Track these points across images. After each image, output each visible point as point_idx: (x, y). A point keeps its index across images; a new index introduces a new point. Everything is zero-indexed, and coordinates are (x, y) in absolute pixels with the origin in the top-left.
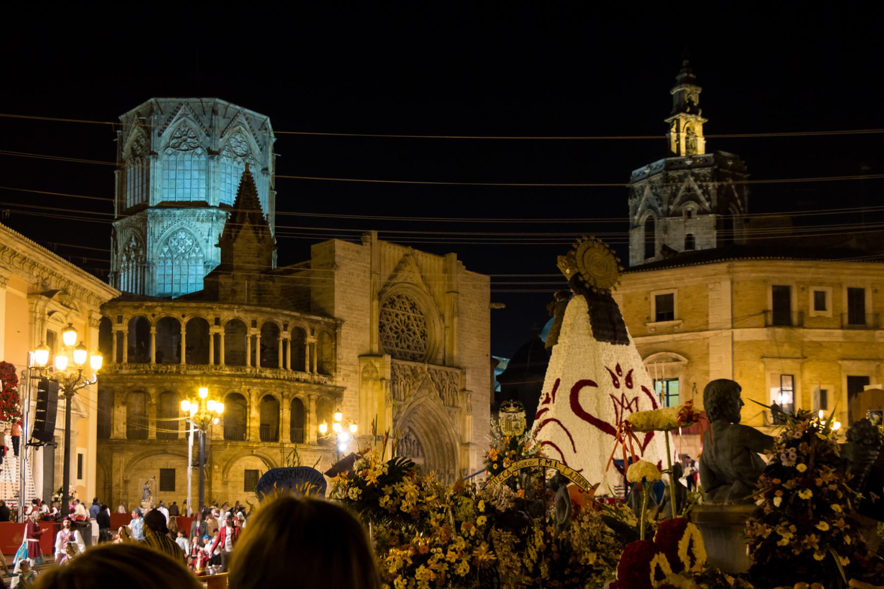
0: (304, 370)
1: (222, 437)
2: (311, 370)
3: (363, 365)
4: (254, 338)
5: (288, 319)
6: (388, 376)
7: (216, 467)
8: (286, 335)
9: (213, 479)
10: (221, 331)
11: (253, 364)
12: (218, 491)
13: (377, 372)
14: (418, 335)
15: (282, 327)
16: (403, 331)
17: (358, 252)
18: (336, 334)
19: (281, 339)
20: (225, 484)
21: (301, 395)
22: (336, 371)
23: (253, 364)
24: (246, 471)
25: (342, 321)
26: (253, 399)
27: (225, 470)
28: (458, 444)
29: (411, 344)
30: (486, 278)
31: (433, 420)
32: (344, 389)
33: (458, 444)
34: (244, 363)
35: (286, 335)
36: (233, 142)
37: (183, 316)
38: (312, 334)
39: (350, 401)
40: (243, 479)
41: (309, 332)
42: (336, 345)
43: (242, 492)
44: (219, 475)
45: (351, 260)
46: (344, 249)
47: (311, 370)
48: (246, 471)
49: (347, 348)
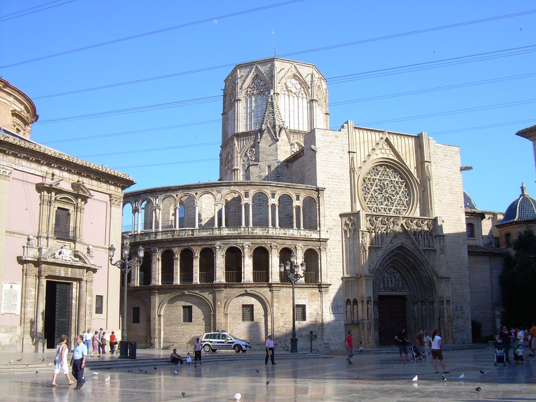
0: (292, 227)
2: (298, 226)
3: (345, 219)
4: (247, 205)
5: (275, 189)
7: (219, 303)
8: (273, 201)
9: (217, 312)
11: (247, 224)
15: (270, 196)
17: (336, 137)
18: (318, 197)
19: (270, 203)
21: (288, 244)
23: (247, 224)
25: (323, 190)
26: (246, 250)
27: (226, 305)
28: (435, 278)
30: (457, 149)
31: (411, 260)
33: (435, 278)
34: (240, 224)
35: (273, 201)
36: (289, 84)
37: (196, 194)
38: (298, 199)
40: (241, 312)
41: (294, 197)
43: (241, 321)
44: (222, 309)
45: (331, 142)
46: (323, 135)
47: (298, 226)
49: (329, 208)
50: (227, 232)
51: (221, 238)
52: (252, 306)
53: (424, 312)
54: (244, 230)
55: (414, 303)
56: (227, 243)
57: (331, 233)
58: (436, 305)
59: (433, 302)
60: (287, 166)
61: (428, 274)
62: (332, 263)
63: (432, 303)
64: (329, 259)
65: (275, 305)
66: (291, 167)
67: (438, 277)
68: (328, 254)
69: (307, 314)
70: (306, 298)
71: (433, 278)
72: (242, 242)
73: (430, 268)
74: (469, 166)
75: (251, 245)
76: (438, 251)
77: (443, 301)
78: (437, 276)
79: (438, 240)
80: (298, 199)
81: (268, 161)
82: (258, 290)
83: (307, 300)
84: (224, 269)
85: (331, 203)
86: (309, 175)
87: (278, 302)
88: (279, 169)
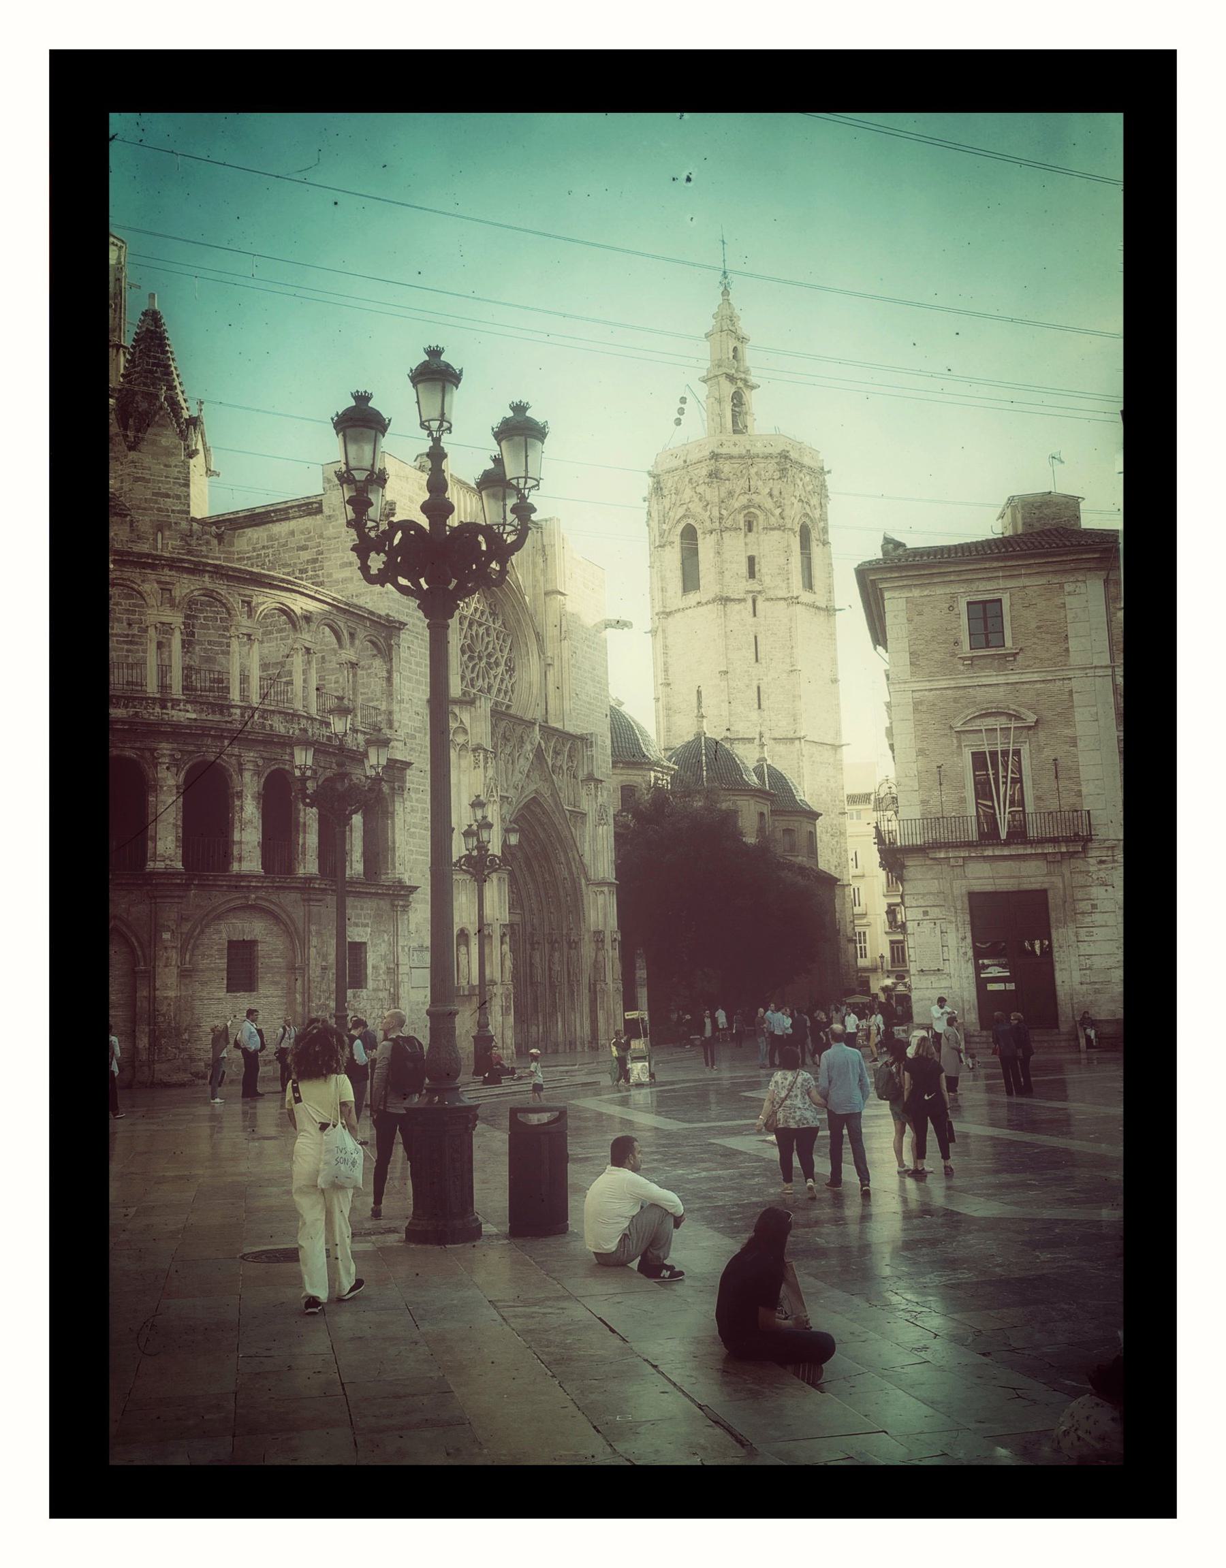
1: (179, 865)
6: (487, 743)
7: (166, 936)
10: (177, 619)
12: (172, 994)
13: (465, 731)
14: (502, 668)
16: (480, 659)
18: (390, 647)
20: (186, 974)
22: (391, 728)
24: (232, 944)
26: (247, 776)
27: (188, 944)
29: (492, 681)
32: (409, 764)
39: (417, 791)
40: (223, 963)
42: (390, 672)
44: (174, 955)
48: (229, 942)
49: (410, 680)
50: (194, 716)
51: (176, 732)
52: (253, 943)
53: (557, 968)
54: (242, 715)
55: (532, 944)
56: (191, 748)
57: (412, 749)
58: (587, 950)
59: (576, 943)
60: (219, 537)
61: (571, 873)
62: (412, 830)
63: (574, 945)
64: (409, 818)
65: (314, 941)
66: (231, 544)
67: (588, 880)
68: (408, 804)
69: (369, 970)
70: (366, 925)
71: (580, 884)
72: (236, 751)
73: (577, 857)
74: (624, 618)
75: (260, 762)
76: (591, 818)
77: (603, 941)
78: (588, 880)
79: (593, 792)
80: (352, 643)
81: (159, 510)
82: (274, 898)
83: (369, 930)
84: (180, 830)
85: (413, 667)
86: (345, 580)
87: (319, 933)
88: (194, 542)
